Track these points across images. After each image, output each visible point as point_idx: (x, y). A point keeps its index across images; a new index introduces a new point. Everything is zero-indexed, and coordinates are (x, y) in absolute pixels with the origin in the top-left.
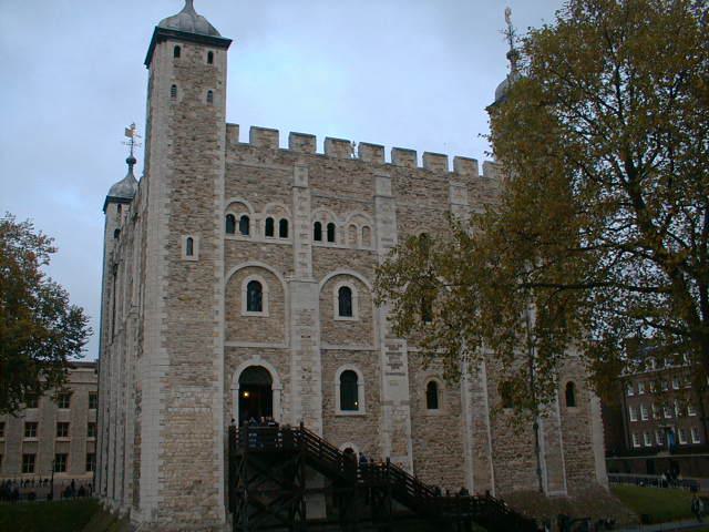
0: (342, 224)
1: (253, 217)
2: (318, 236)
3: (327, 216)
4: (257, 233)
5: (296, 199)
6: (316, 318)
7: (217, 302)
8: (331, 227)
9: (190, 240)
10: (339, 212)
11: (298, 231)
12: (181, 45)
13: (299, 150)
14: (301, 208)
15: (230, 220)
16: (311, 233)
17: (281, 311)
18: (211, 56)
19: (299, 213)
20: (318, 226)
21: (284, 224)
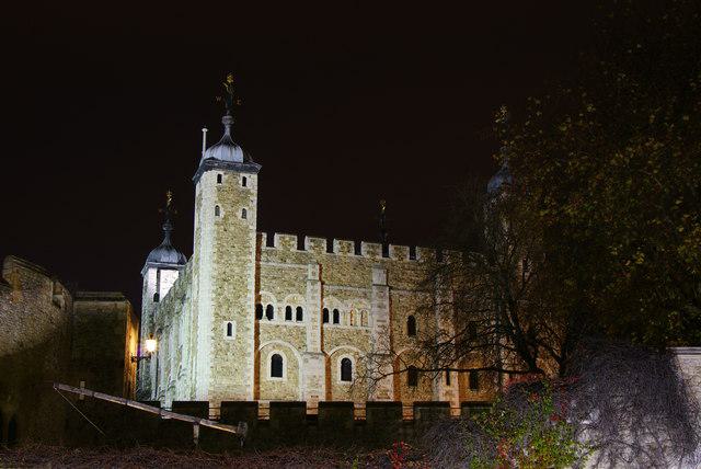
0: (345, 309)
1: (275, 306)
2: (325, 319)
3: (332, 303)
4: (279, 317)
5: (309, 290)
6: (323, 382)
7: (248, 370)
8: (336, 313)
9: (229, 326)
10: (342, 299)
11: (311, 316)
12: (221, 173)
13: (312, 251)
14: (313, 298)
15: (259, 309)
16: (319, 317)
17: (296, 377)
18: (245, 179)
19: (312, 302)
20: (325, 313)
21: (299, 310)
